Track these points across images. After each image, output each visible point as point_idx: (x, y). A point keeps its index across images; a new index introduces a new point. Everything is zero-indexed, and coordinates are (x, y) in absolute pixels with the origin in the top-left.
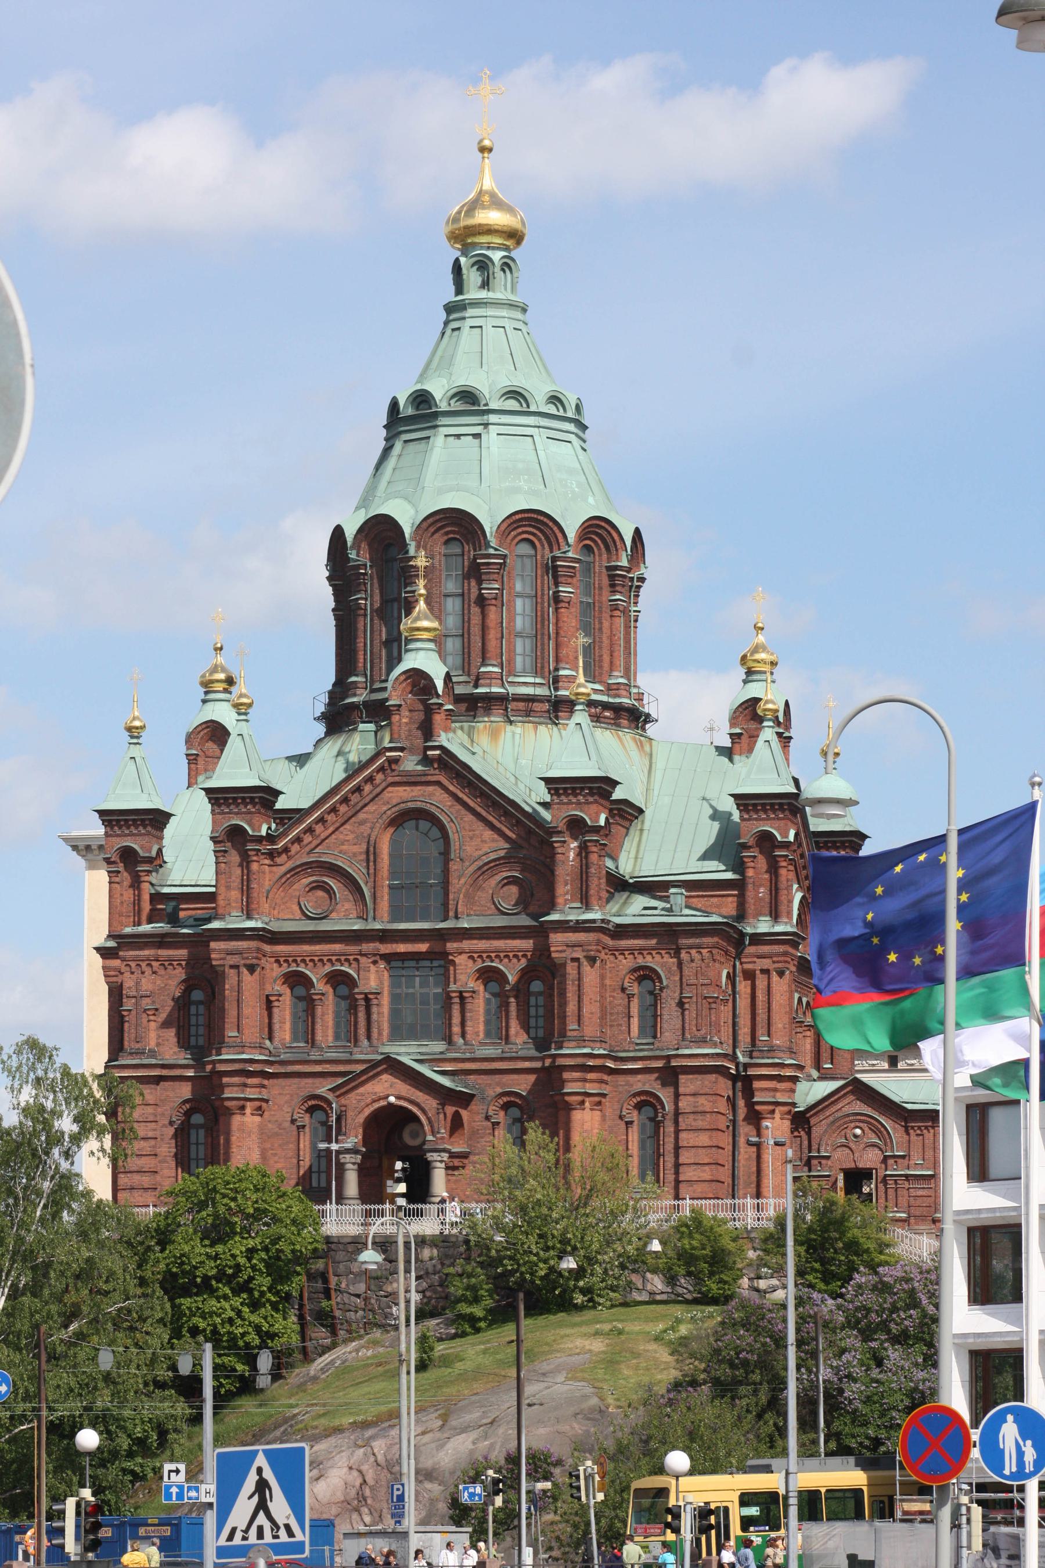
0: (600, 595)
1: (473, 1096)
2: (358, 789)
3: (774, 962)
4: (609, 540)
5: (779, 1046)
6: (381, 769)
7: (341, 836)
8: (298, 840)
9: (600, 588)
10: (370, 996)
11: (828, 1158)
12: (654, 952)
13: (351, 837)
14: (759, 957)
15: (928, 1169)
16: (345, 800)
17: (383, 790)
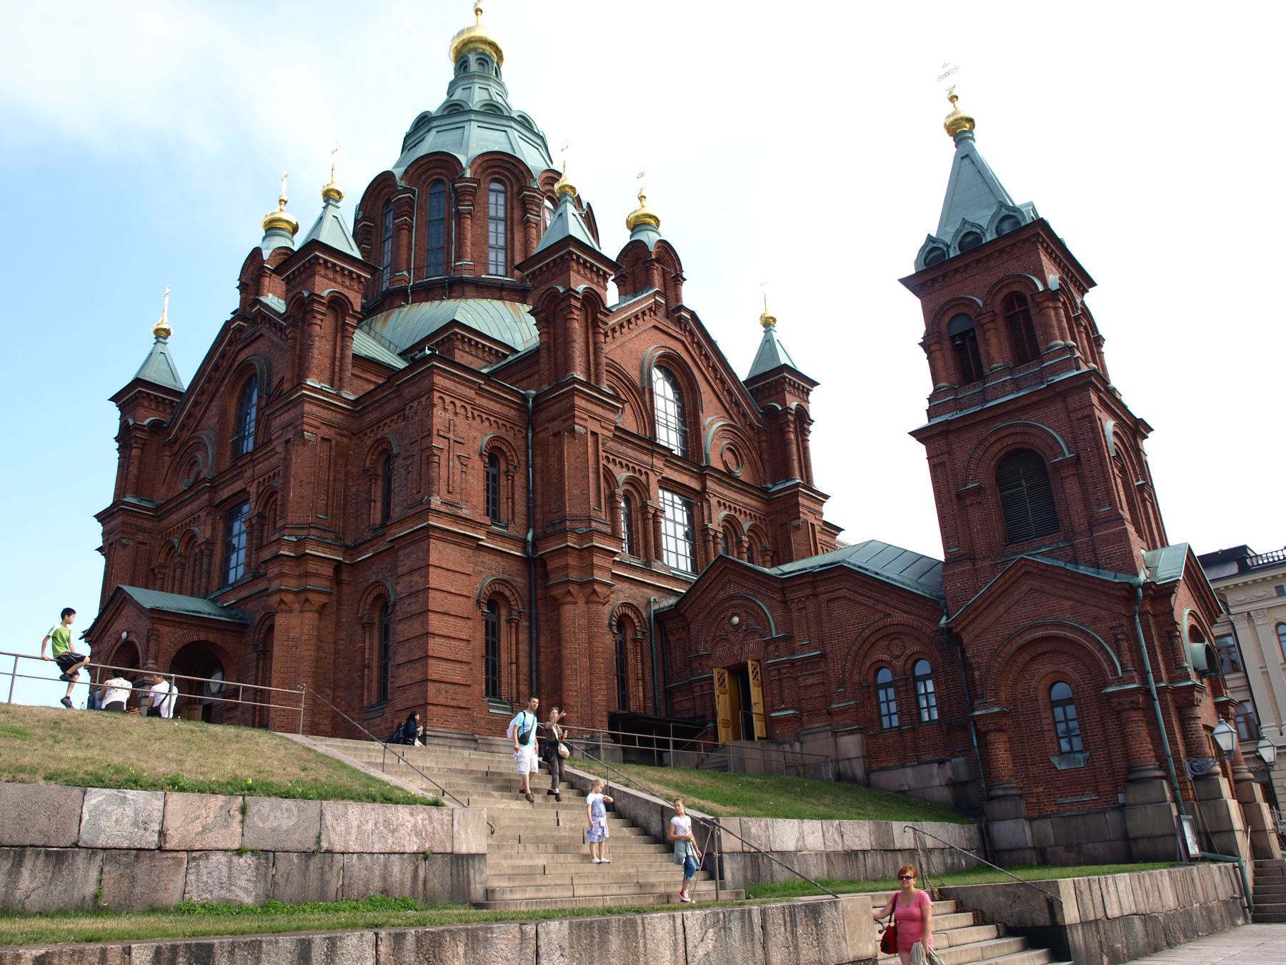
0: (512, 213)
1: (247, 626)
2: (216, 368)
3: (564, 421)
4: (516, 171)
5: (576, 516)
6: (230, 343)
7: (210, 413)
8: (183, 427)
9: (512, 208)
10: (203, 548)
11: (708, 656)
12: (388, 421)
13: (215, 409)
14: (549, 421)
15: (816, 649)
16: (209, 380)
17: (234, 361)
